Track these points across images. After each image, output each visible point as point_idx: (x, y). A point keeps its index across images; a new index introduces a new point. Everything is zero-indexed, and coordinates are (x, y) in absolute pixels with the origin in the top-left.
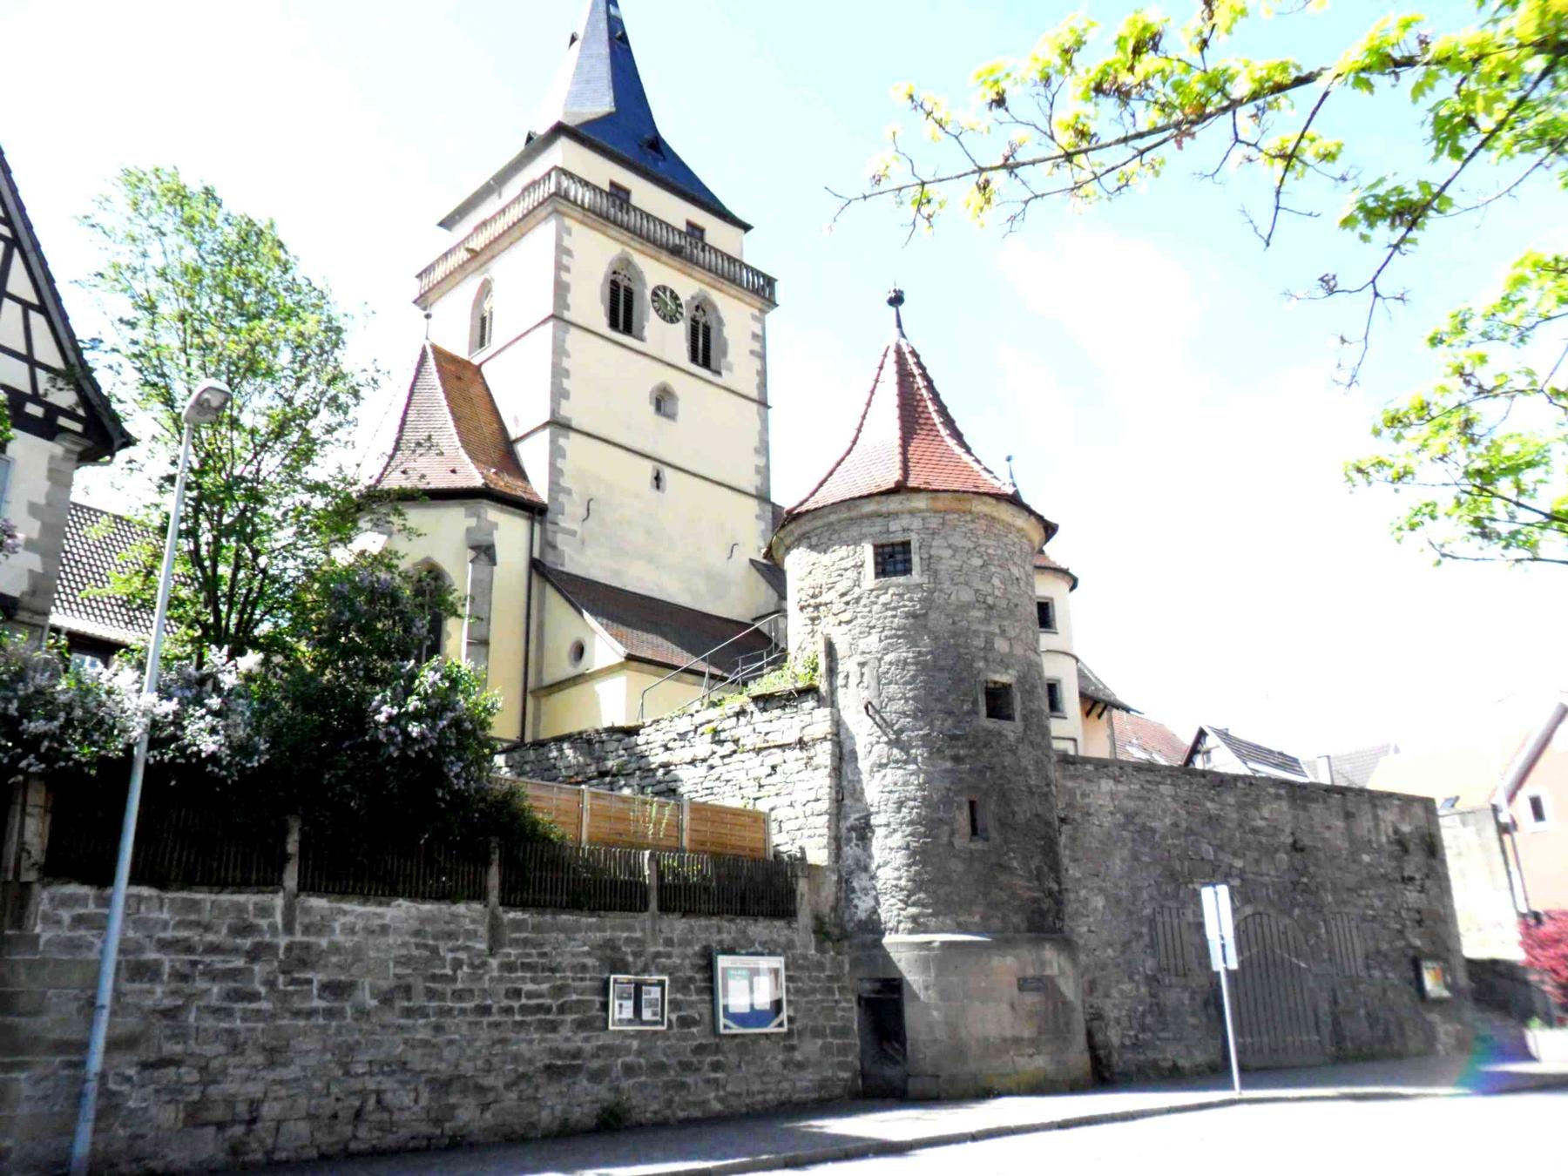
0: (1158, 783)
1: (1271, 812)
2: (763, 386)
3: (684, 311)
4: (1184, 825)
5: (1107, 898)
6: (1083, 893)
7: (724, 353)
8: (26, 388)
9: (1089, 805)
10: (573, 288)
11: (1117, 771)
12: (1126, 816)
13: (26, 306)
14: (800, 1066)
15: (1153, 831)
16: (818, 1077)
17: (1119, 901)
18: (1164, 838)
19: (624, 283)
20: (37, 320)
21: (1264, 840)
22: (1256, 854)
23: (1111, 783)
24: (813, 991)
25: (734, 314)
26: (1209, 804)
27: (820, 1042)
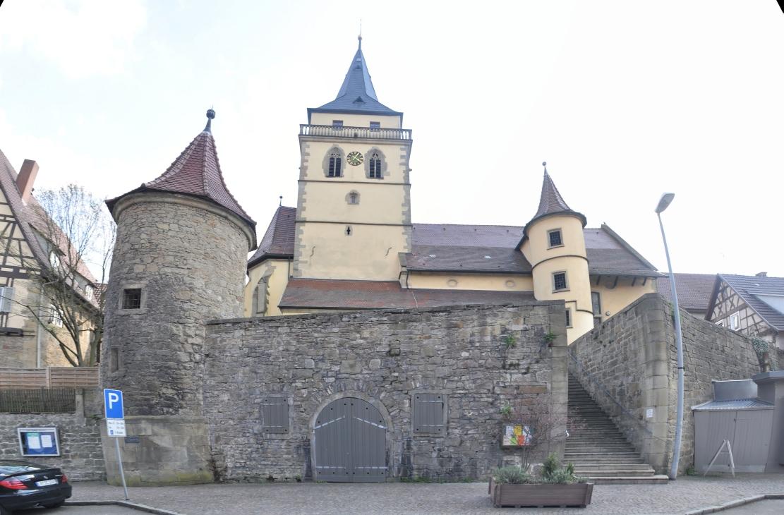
0: (278, 327)
1: (371, 333)
2: (407, 177)
3: (364, 158)
4: (293, 348)
5: (231, 395)
6: (216, 393)
7: (386, 169)
8: (20, 265)
9: (225, 346)
10: (309, 168)
11: (247, 324)
12: (251, 348)
13: (19, 240)
14: (73, 468)
15: (269, 355)
16: (83, 472)
17: (239, 396)
18: (277, 358)
19: (375, 159)
20: (24, 244)
21: (361, 352)
22: (352, 362)
23: (242, 332)
24: (84, 440)
25: (391, 154)
26: (316, 335)
27: (85, 460)
